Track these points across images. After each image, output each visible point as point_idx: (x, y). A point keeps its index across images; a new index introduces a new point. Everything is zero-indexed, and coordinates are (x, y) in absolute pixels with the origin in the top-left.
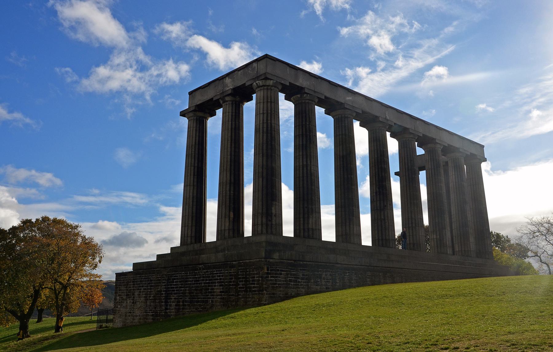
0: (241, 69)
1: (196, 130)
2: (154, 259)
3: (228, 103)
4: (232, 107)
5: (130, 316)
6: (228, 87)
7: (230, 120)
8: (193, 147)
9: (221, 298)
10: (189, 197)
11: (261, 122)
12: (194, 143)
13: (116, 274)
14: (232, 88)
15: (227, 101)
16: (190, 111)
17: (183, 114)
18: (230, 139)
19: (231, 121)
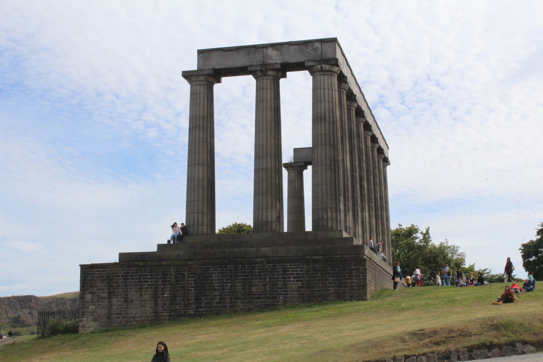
0: (296, 44)
1: (207, 98)
2: (154, 249)
3: (269, 78)
4: (274, 83)
5: (119, 318)
6: (271, 59)
7: (273, 98)
8: (205, 118)
9: (300, 294)
10: (203, 179)
11: (327, 110)
12: (206, 114)
13: (80, 265)
14: (279, 62)
15: (269, 76)
16: (201, 73)
17: (187, 75)
18: (273, 119)
19: (274, 100)
